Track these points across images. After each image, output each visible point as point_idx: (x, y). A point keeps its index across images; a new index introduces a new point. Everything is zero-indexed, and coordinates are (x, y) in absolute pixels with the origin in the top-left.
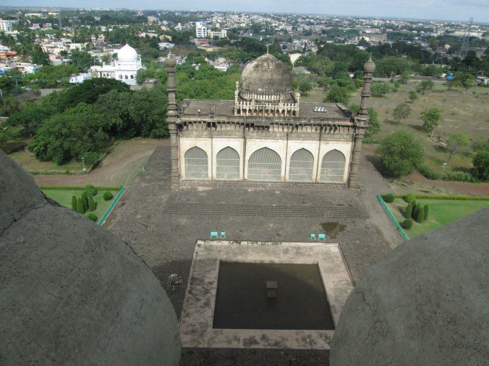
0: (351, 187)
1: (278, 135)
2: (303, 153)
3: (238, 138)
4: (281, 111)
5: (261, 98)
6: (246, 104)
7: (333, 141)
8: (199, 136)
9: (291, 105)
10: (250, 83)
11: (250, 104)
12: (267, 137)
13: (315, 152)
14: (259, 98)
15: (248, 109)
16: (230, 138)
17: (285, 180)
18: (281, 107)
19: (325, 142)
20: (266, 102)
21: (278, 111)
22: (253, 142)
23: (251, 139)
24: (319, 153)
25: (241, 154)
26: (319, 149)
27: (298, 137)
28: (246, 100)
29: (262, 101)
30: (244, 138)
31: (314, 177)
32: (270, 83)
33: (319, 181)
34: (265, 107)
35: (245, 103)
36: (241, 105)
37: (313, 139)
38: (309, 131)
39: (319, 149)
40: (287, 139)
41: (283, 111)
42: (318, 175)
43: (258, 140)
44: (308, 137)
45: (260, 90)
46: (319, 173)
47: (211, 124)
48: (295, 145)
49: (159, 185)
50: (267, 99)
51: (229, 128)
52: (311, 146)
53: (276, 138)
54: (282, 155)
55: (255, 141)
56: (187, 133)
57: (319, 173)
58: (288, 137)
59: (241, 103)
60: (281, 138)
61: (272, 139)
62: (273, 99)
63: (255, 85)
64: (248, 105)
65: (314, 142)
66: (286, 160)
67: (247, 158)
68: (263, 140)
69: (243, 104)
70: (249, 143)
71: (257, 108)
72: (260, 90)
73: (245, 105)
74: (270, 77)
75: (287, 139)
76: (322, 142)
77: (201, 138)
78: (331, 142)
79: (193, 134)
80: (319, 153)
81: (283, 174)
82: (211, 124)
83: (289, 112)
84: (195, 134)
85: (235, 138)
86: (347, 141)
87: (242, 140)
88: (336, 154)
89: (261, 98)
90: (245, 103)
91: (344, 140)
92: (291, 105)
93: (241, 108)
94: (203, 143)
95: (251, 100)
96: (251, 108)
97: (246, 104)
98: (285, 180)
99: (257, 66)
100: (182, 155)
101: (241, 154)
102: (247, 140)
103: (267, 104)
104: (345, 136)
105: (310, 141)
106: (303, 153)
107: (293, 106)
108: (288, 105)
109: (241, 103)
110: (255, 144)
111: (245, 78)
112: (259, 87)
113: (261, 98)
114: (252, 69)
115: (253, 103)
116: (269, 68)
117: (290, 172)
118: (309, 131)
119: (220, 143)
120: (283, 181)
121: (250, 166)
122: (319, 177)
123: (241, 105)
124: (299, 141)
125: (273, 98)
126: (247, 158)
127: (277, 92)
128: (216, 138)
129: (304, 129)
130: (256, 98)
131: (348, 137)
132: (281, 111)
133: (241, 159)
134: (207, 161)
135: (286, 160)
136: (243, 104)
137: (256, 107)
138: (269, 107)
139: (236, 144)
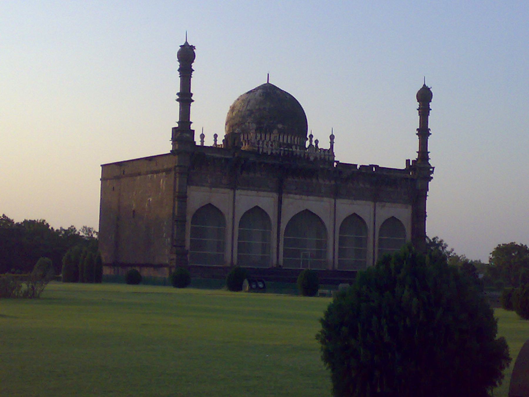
2: (355, 219)
3: (271, 191)
4: (312, 158)
12: (308, 193)
29: (284, 144)
34: (293, 152)
43: (297, 197)
52: (364, 208)
54: (328, 223)
67: (283, 227)
71: (282, 152)
78: (388, 204)
87: (276, 195)
94: (221, 198)
96: (274, 152)
100: (189, 218)
102: (283, 195)
110: (294, 204)
119: (247, 199)
123: (260, 146)
126: (283, 227)
133: (275, 230)
139: (266, 201)
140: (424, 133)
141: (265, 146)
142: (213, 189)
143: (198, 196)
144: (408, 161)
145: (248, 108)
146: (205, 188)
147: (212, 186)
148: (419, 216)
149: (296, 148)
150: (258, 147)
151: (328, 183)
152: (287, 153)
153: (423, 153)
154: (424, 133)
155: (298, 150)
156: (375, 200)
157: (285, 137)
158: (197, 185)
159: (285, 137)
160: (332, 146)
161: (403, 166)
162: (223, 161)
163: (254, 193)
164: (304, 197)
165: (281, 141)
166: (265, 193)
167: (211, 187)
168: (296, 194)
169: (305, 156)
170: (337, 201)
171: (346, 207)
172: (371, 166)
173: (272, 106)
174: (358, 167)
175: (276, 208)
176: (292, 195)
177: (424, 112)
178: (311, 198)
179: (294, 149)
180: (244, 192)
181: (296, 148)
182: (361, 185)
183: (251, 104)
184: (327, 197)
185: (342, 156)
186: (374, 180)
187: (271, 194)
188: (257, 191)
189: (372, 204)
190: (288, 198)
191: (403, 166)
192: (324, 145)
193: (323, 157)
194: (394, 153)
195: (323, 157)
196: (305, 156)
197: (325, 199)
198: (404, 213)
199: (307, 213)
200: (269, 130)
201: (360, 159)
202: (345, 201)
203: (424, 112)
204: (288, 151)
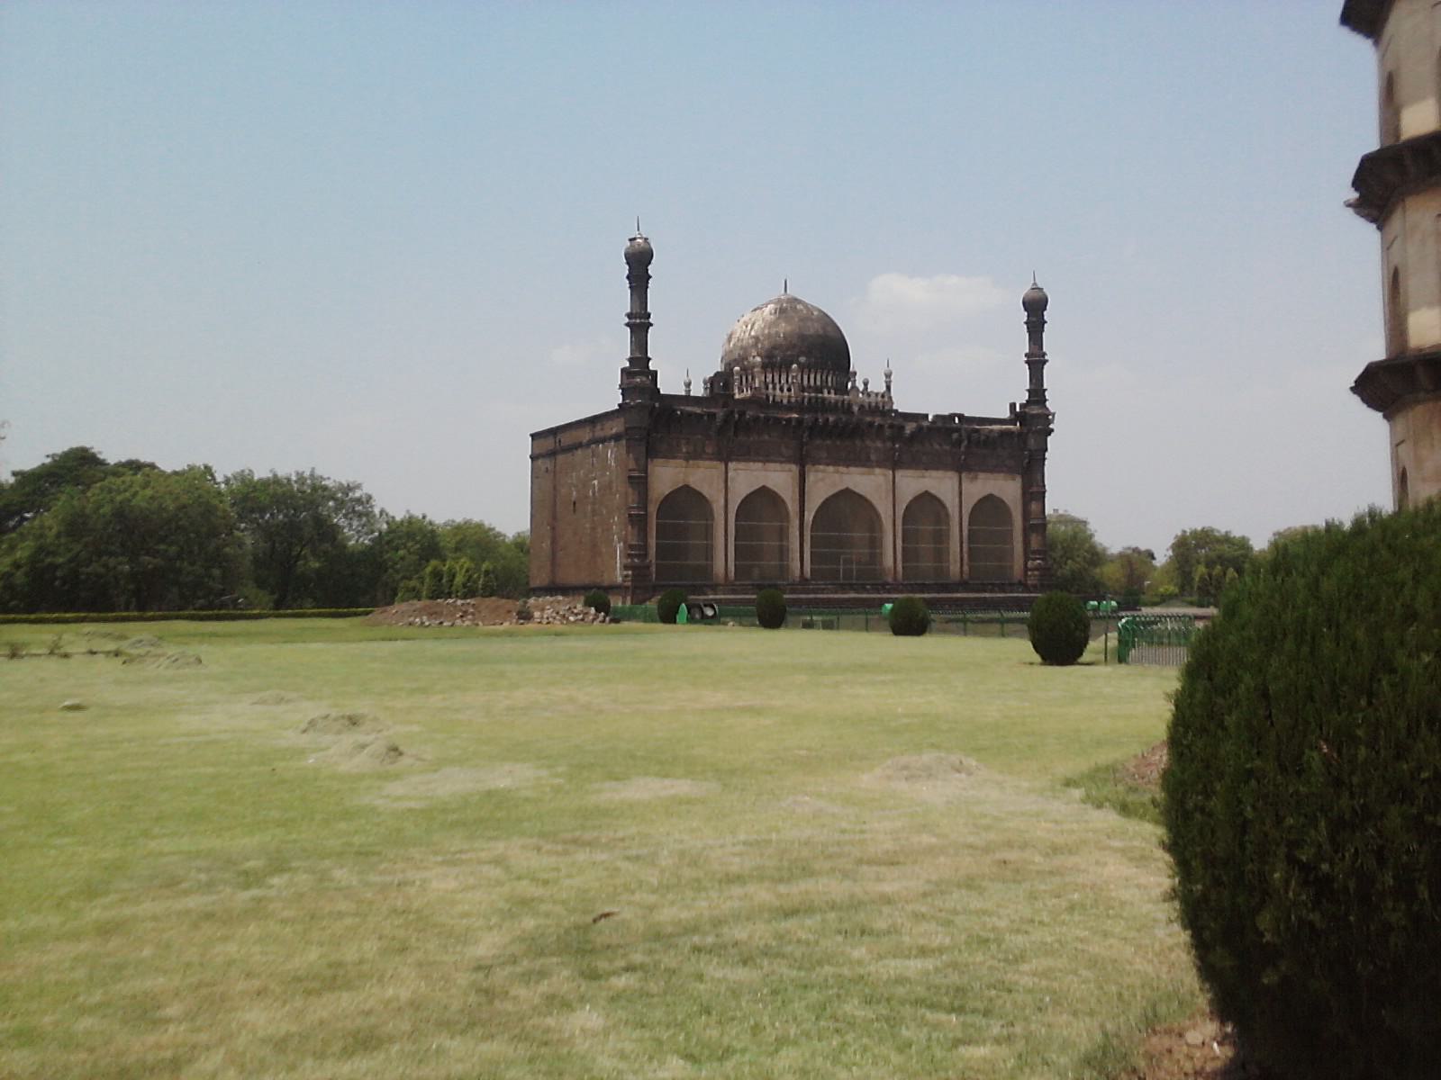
1: (873, 457)
2: (926, 504)
12: (849, 462)
19: (972, 475)
22: (820, 475)
25: (792, 507)
26: (961, 493)
34: (824, 399)
39: (961, 493)
43: (831, 469)
44: (935, 464)
52: (942, 484)
54: (883, 508)
55: (823, 471)
60: (880, 464)
70: (811, 478)
71: (806, 400)
74: (821, 332)
77: (701, 463)
78: (981, 475)
84: (684, 450)
87: (795, 468)
94: (704, 477)
100: (653, 509)
101: (792, 507)
106: (926, 504)
110: (826, 482)
117: (904, 561)
119: (747, 477)
123: (770, 391)
135: (894, 521)
139: (779, 478)
140: (1036, 362)
141: (778, 392)
142: (691, 462)
143: (666, 476)
144: (1013, 406)
145: (753, 333)
146: (678, 461)
147: (689, 457)
148: (1034, 492)
151: (879, 444)
152: (813, 401)
153: (1037, 393)
154: (1036, 362)
155: (833, 396)
159: (812, 376)
160: (888, 388)
161: (1006, 414)
162: (706, 418)
163: (760, 465)
164: (842, 469)
165: (805, 382)
166: (777, 466)
167: (687, 460)
168: (828, 465)
170: (899, 474)
171: (912, 483)
172: (952, 416)
173: (789, 328)
174: (930, 418)
175: (797, 490)
176: (821, 467)
177: (1036, 326)
178: (852, 469)
179: (826, 395)
180: (742, 465)
181: (829, 393)
182: (937, 447)
183: (756, 327)
184: (880, 467)
185: (902, 404)
186: (956, 441)
187: (787, 466)
190: (817, 471)
191: (1006, 414)
192: (877, 386)
194: (993, 395)
197: (878, 471)
198: (1008, 489)
199: (847, 494)
200: (784, 366)
201: (933, 406)
202: (910, 472)
203: (1036, 326)
204: (817, 398)
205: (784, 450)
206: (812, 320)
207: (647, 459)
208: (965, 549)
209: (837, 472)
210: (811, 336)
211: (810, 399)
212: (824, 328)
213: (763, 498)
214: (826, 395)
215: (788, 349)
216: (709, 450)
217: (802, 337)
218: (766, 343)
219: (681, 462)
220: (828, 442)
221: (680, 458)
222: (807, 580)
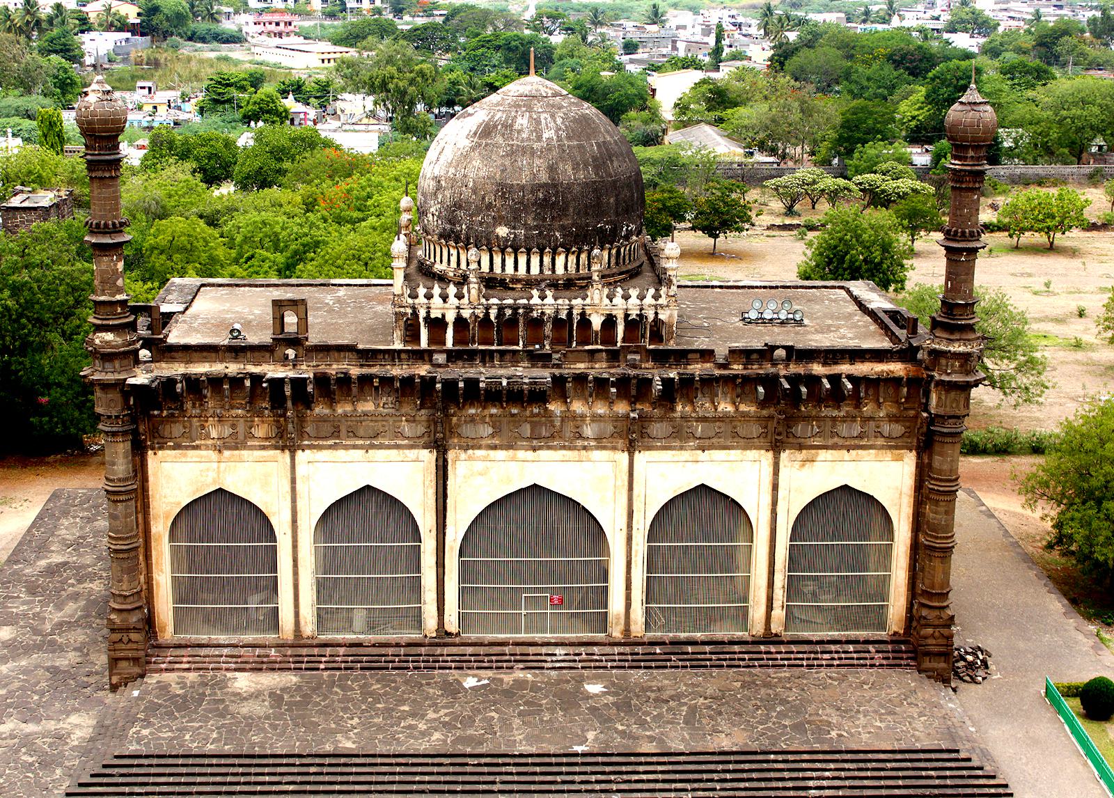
0: (928, 654)
1: (588, 431)
2: (705, 508)
4: (597, 322)
5: (510, 269)
6: (444, 298)
7: (834, 447)
8: (234, 443)
9: (641, 297)
10: (458, 205)
11: (459, 296)
13: (755, 505)
14: (498, 270)
15: (451, 317)
16: (373, 447)
17: (627, 631)
18: (598, 304)
20: (530, 283)
21: (585, 322)
22: (478, 466)
23: (466, 448)
24: (774, 503)
25: (426, 521)
26: (775, 487)
27: (679, 436)
28: (442, 279)
29: (515, 280)
30: (440, 448)
31: (757, 613)
32: (544, 204)
33: (776, 628)
34: (529, 308)
35: (437, 290)
36: (422, 299)
37: (747, 443)
38: (725, 407)
39: (775, 487)
40: (631, 449)
41: (610, 322)
42: (777, 603)
44: (726, 435)
45: (502, 231)
46: (779, 595)
47: (288, 391)
48: (668, 472)
49: (54, 671)
50: (535, 270)
51: (368, 406)
52: (739, 472)
53: (579, 443)
55: (485, 459)
56: (177, 429)
57: (779, 595)
58: (633, 437)
59: (422, 291)
60: (601, 443)
61: (564, 448)
62: (560, 270)
63: (479, 211)
64: (453, 301)
65: (752, 454)
66: (629, 539)
68: (521, 454)
69: (429, 296)
71: (493, 313)
72: (502, 231)
73: (437, 301)
74: (544, 177)
75: (631, 449)
76: (785, 456)
77: (245, 453)
78: (823, 454)
79: (208, 436)
80: (774, 503)
81: (616, 605)
82: (288, 391)
83: (633, 325)
84: (214, 434)
85: (398, 447)
86: (895, 445)
87: (428, 457)
88: (846, 508)
89: (510, 269)
90: (437, 290)
91: (880, 442)
92: (641, 297)
93: (422, 313)
94: (255, 474)
95: (463, 281)
96: (466, 314)
97: (444, 298)
98: (627, 631)
99: (487, 131)
100: (160, 528)
101: (426, 521)
102: (451, 455)
103: (535, 293)
104: (886, 428)
105: (735, 454)
106: (705, 508)
107: (649, 300)
108: (626, 297)
109: (422, 291)
110: (488, 473)
111: (438, 180)
112: (499, 220)
113: (508, 266)
114: (465, 143)
115: (474, 287)
116: (539, 138)
117: (649, 596)
118: (725, 407)
119: (331, 472)
120: (617, 633)
121: (466, 572)
122: (778, 613)
123: (422, 299)
124: (686, 455)
125: (562, 265)
127: (578, 240)
128: (311, 447)
129: (704, 406)
130: (485, 267)
131: (898, 429)
132: (597, 322)
134: (274, 550)
135: (629, 539)
136: (429, 296)
137: (488, 308)
138: (547, 304)
139: (402, 472)
142: (227, 453)
146: (203, 453)
147: (223, 445)
149: (543, 297)
150: (414, 308)
151: (601, 409)
152: (508, 312)
155: (549, 300)
156: (776, 447)
157: (522, 260)
158: (177, 447)
159: (522, 260)
162: (248, 383)
163: (359, 453)
168: (495, 448)
169: (570, 314)
170: (640, 457)
175: (431, 491)
176: (478, 453)
178: (544, 454)
179: (536, 300)
181: (543, 297)
188: (367, 448)
189: (766, 457)
190: (470, 459)
193: (634, 313)
195: (634, 313)
196: (570, 314)
198: (888, 476)
205: (406, 428)
206: (533, 153)
207: (139, 451)
208: (780, 580)
209: (513, 459)
210: (522, 188)
211: (501, 309)
212: (552, 169)
213: (367, 504)
214: (536, 300)
215: (479, 211)
216: (261, 431)
217: (504, 190)
218: (448, 193)
219: (212, 455)
220: (494, 411)
221: (207, 448)
222: (449, 634)
